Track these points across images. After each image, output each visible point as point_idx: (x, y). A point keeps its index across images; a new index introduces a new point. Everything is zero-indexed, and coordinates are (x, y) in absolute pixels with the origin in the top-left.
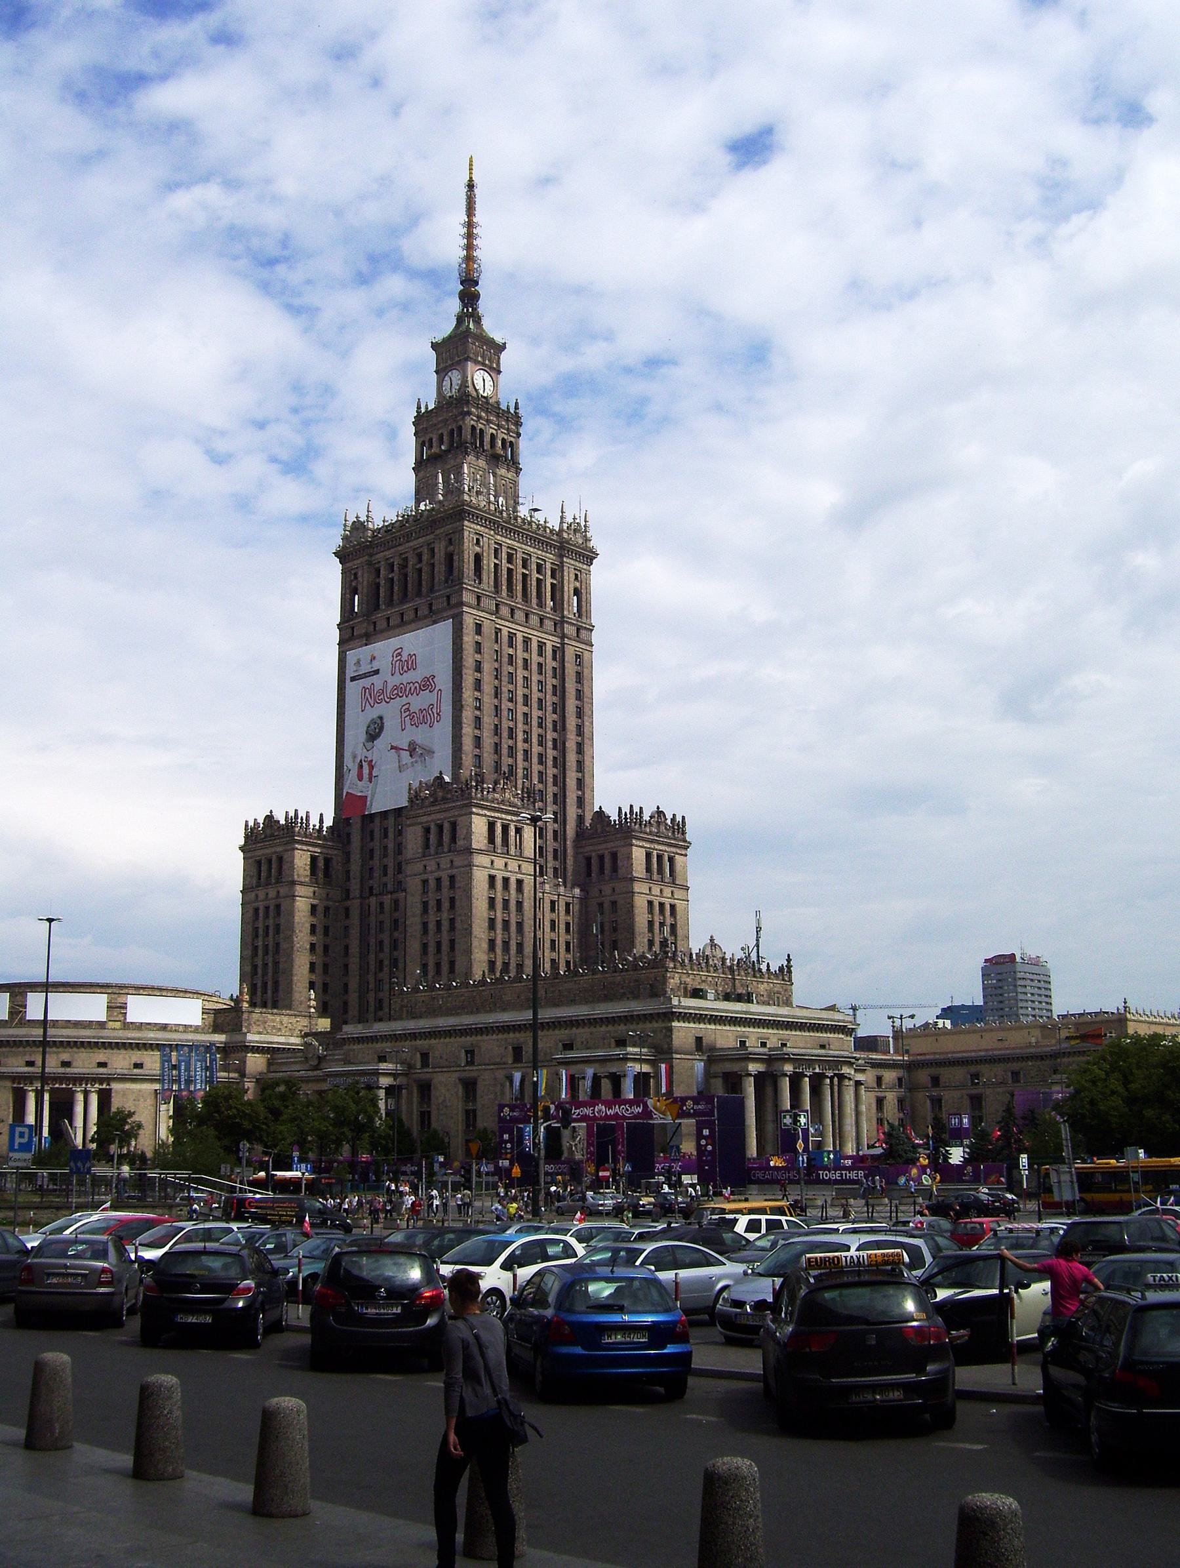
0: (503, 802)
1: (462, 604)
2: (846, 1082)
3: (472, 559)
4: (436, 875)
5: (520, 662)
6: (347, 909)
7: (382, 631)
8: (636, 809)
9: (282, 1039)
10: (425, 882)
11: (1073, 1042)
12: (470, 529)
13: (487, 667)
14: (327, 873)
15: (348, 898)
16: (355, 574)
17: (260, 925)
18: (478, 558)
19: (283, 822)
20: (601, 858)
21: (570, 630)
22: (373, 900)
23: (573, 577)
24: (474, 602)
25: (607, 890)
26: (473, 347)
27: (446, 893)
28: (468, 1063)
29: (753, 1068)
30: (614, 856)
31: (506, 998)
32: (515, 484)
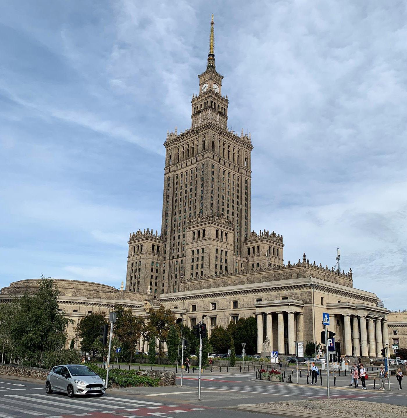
0: (222, 223)
4: (197, 248)
6: (164, 264)
8: (266, 231)
9: (136, 302)
10: (193, 251)
13: (216, 180)
15: (165, 260)
16: (171, 151)
17: (134, 269)
18: (213, 142)
19: (143, 233)
20: (254, 248)
22: (174, 260)
23: (245, 153)
24: (212, 157)
25: (255, 259)
27: (200, 255)
28: (213, 309)
29: (351, 312)
30: (258, 247)
32: (226, 123)
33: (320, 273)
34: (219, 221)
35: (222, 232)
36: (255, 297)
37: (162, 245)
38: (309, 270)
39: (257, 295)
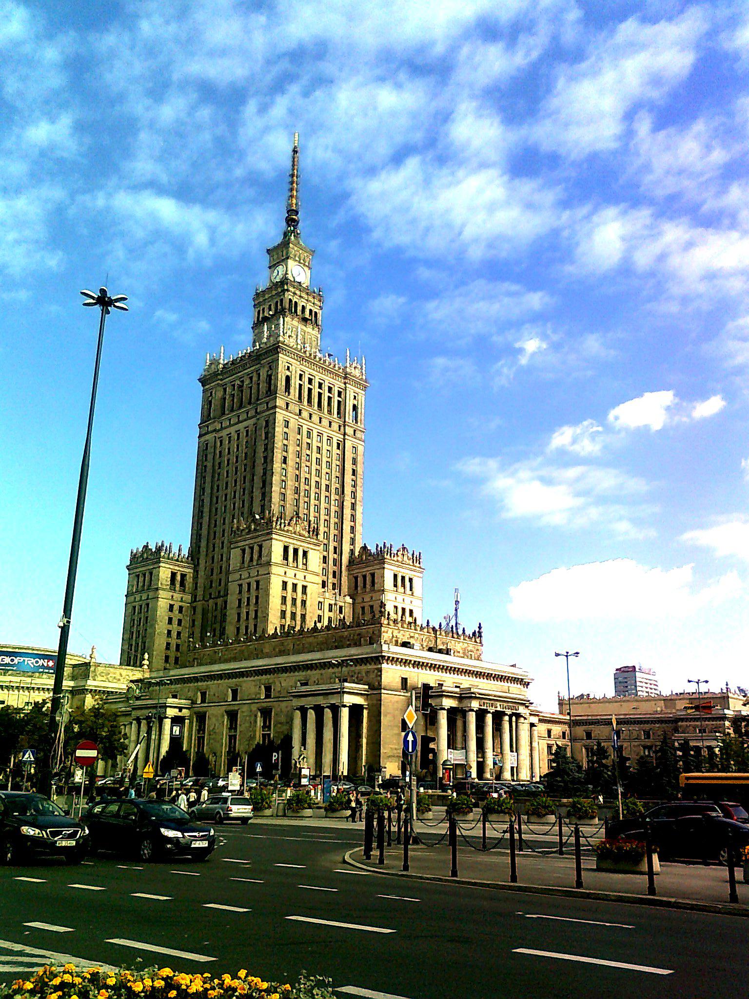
0: (295, 533)
1: (275, 407)
2: (522, 720)
3: (284, 378)
5: (315, 449)
7: (225, 428)
8: (388, 545)
10: (240, 586)
11: (689, 711)
12: (283, 359)
13: (291, 449)
14: (182, 584)
15: (195, 601)
18: (288, 379)
20: (364, 577)
21: (349, 431)
22: (211, 601)
25: (367, 599)
26: (293, 249)
29: (448, 703)
30: (373, 575)
31: (266, 650)
33: (412, 635)
34: (291, 528)
35: (296, 551)
36: (298, 678)
37: (189, 571)
38: (390, 631)
39: (301, 675)
